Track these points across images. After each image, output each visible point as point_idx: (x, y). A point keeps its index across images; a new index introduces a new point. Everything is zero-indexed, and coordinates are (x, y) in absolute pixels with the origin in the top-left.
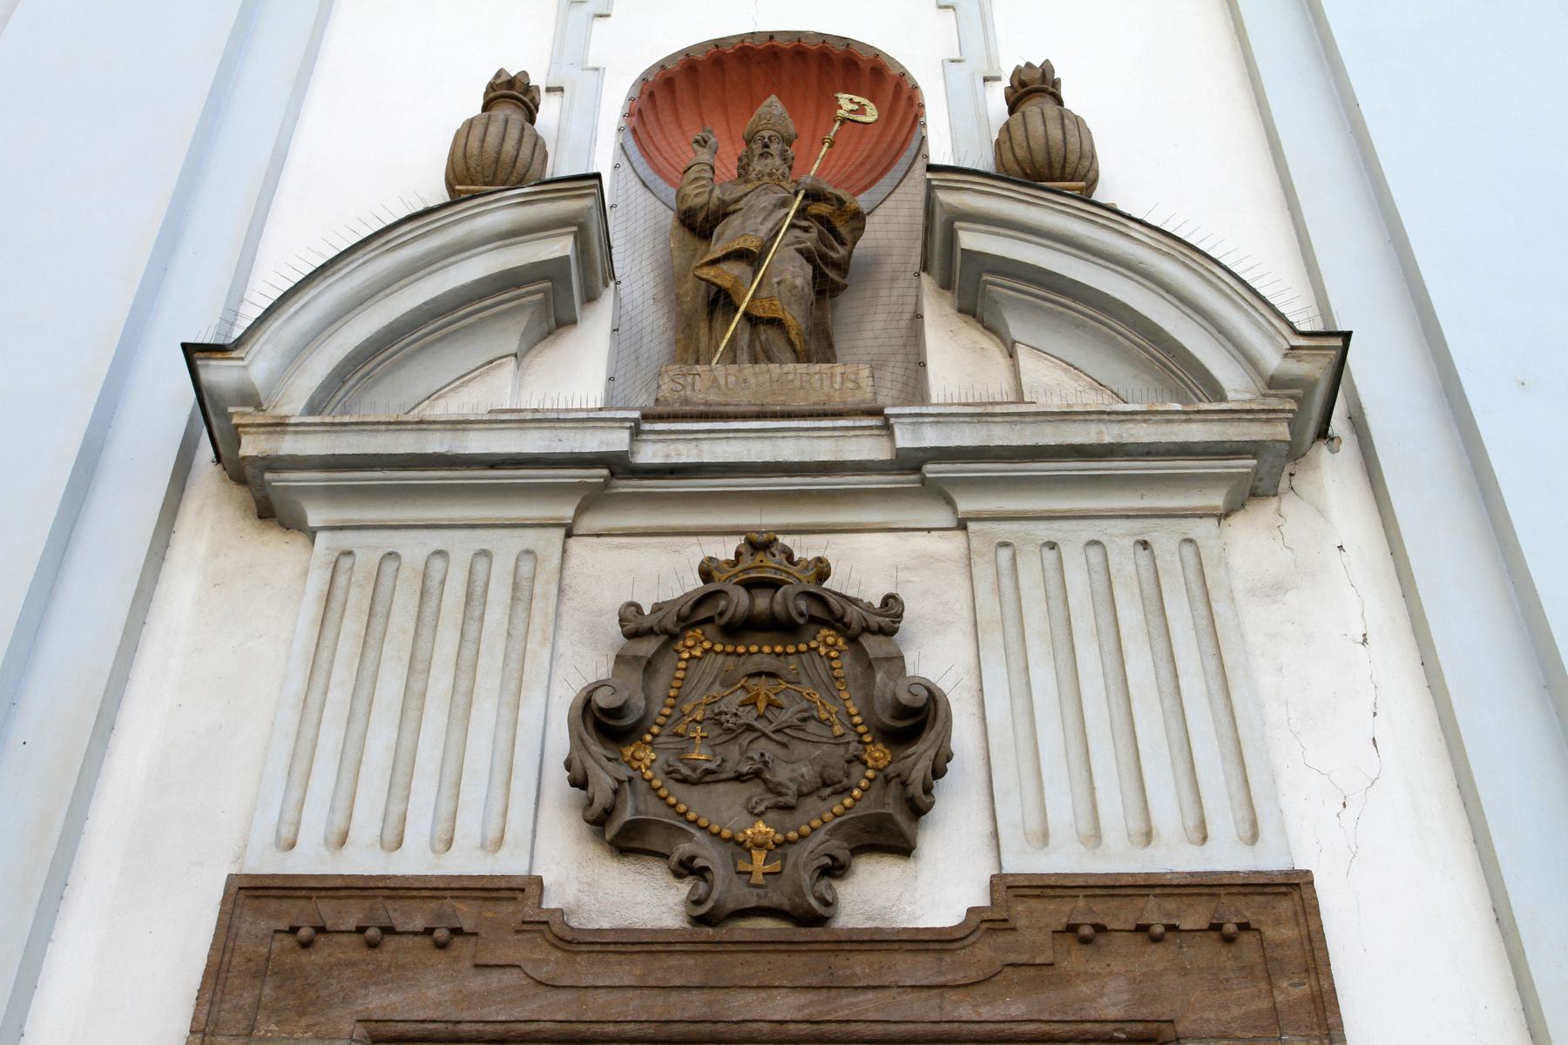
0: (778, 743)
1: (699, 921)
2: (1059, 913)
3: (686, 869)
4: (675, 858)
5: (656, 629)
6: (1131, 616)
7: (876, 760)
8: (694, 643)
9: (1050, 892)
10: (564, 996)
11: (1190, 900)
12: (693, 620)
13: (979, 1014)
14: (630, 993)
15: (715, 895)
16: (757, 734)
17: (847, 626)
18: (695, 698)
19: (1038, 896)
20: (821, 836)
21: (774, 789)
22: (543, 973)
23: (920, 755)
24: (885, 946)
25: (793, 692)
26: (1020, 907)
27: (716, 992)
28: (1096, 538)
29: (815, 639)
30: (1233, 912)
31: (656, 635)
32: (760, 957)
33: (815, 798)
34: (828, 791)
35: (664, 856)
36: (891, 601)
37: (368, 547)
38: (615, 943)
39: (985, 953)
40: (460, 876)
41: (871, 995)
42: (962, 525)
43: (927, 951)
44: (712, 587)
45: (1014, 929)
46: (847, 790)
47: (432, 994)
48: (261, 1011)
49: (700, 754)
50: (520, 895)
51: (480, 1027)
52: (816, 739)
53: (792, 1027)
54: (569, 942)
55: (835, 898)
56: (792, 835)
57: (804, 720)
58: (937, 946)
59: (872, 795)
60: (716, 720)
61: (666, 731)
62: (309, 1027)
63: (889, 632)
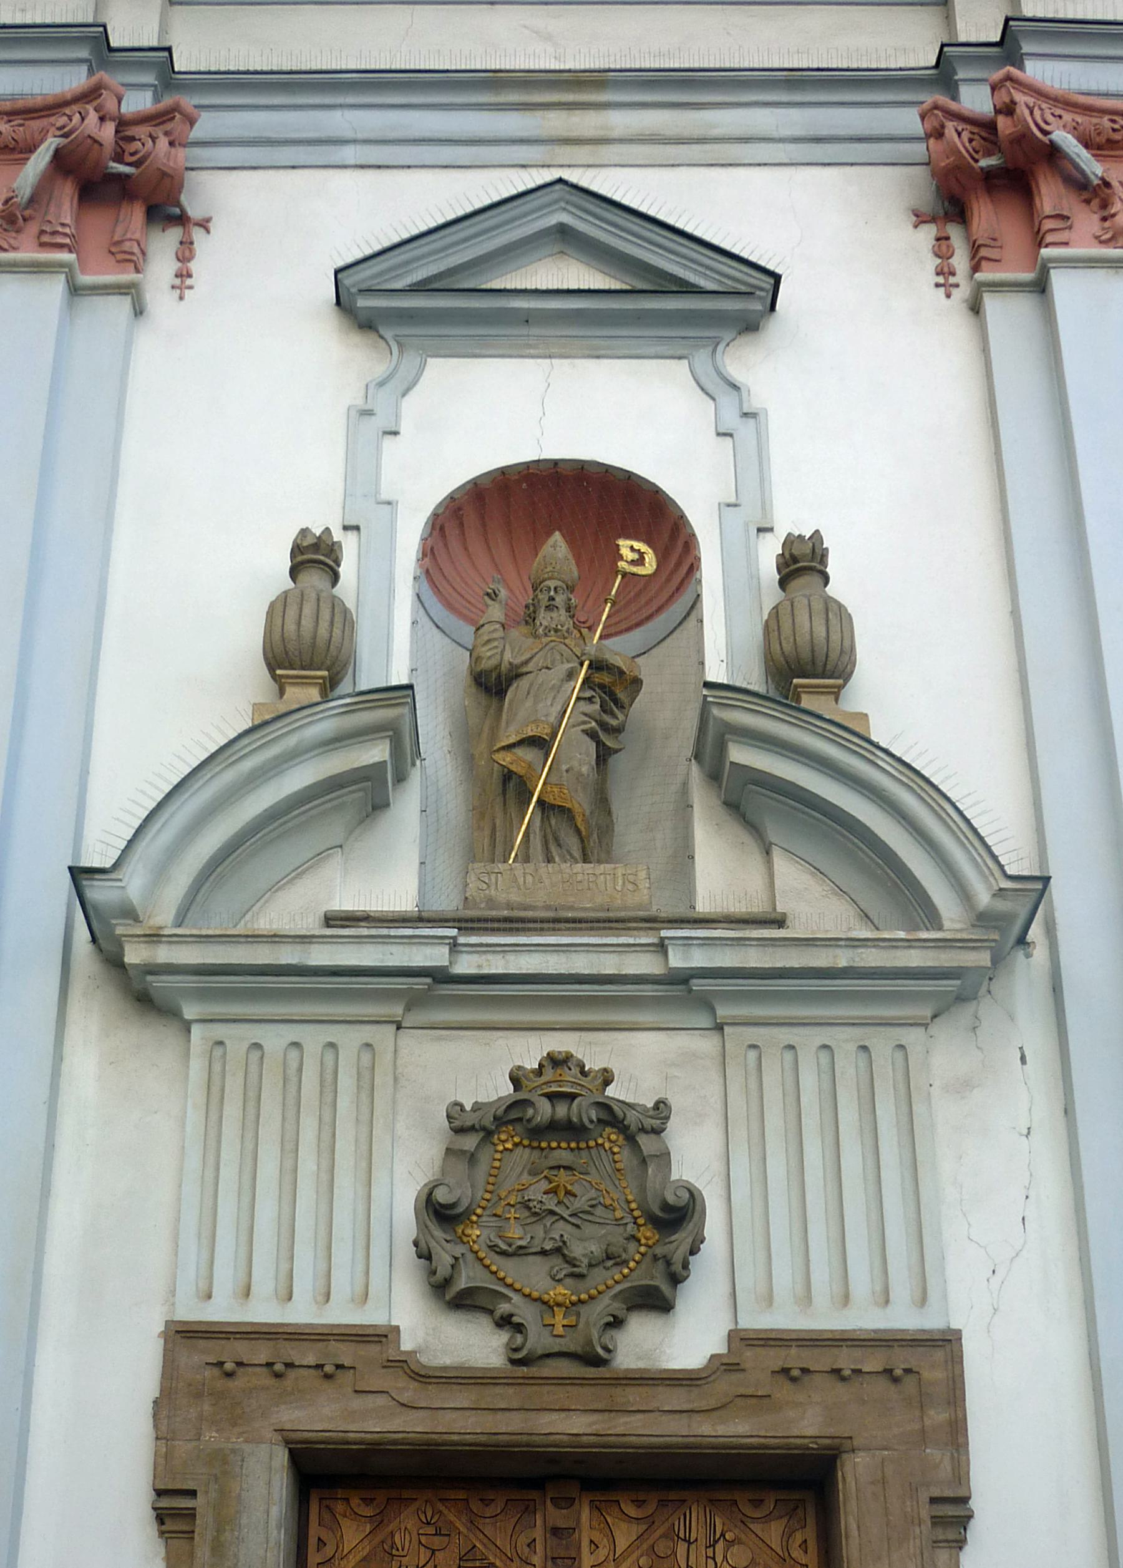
0: (573, 1224)
1: (513, 1362)
2: (775, 1359)
3: (505, 1322)
4: (498, 1314)
5: (477, 1126)
6: (849, 1115)
7: (647, 1239)
8: (506, 1139)
9: (772, 1343)
10: (421, 1414)
11: (870, 1350)
12: (505, 1120)
13: (716, 1431)
14: (468, 1413)
15: (528, 1345)
16: (557, 1217)
17: (627, 1128)
18: (508, 1185)
19: (763, 1346)
20: (606, 1300)
21: (571, 1262)
22: (405, 1398)
23: (682, 1238)
24: (651, 1382)
25: (584, 1182)
26: (748, 1353)
27: (530, 1413)
28: (828, 1043)
29: (601, 1136)
30: (900, 1360)
31: (477, 1131)
32: (561, 1388)
33: (601, 1267)
34: (610, 1263)
35: (491, 1312)
36: (662, 1105)
37: (238, 1037)
38: (457, 1377)
39: (725, 1386)
40: (339, 1325)
41: (640, 1416)
42: (719, 1028)
43: (681, 1385)
44: (521, 1096)
45: (743, 1370)
46: (625, 1263)
47: (326, 1411)
48: (204, 1422)
49: (515, 1232)
50: (384, 1340)
51: (363, 1435)
52: (602, 1221)
53: (585, 1438)
54: (423, 1376)
55: (615, 1347)
56: (584, 1296)
57: (592, 1206)
58: (688, 1382)
59: (643, 1266)
60: (526, 1205)
61: (488, 1212)
62: (240, 1434)
63: (657, 1132)
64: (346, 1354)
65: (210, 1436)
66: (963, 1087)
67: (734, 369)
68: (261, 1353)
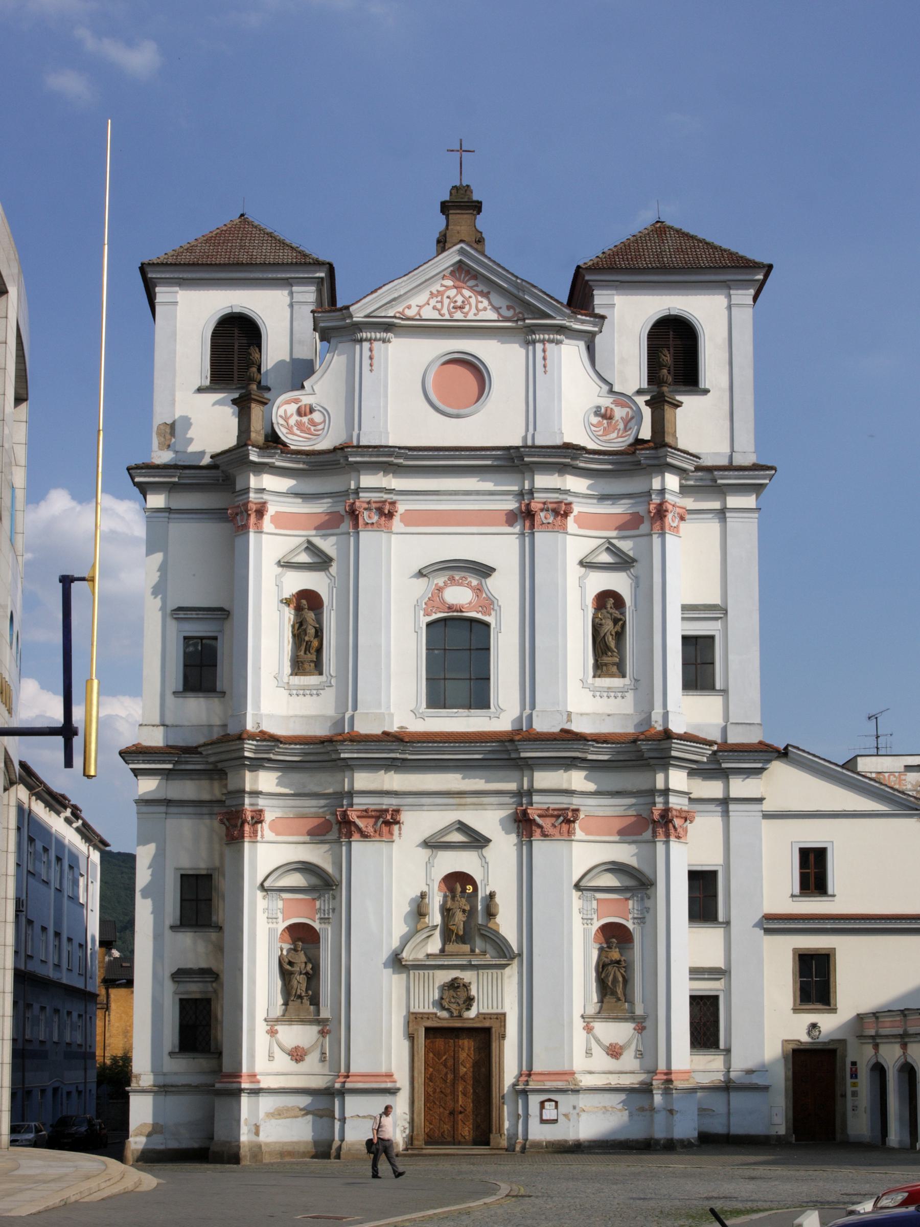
39: (477, 1019)
60: (453, 997)
65: (415, 1027)
68: (421, 1016)
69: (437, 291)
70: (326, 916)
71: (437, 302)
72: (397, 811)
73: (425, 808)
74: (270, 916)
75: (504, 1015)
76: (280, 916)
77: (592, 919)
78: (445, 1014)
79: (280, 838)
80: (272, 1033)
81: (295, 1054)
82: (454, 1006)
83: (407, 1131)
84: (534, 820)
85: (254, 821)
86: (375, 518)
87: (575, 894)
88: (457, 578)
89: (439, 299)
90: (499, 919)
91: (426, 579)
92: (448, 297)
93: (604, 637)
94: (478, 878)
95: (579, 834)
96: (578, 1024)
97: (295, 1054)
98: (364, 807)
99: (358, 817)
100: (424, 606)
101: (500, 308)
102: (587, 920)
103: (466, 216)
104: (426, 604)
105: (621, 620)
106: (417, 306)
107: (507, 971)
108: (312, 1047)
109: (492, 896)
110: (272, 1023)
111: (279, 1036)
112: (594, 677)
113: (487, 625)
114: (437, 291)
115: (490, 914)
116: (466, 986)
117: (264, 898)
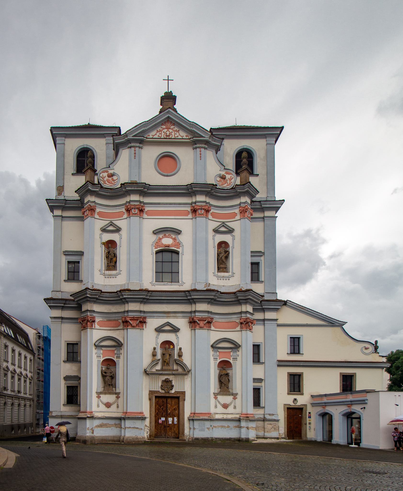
30: (183, 393)
39: (175, 394)
64: (157, 392)
66: (187, 378)
67: (177, 334)
69: (160, 130)
70: (118, 356)
71: (160, 134)
72: (145, 318)
73: (155, 317)
74: (98, 356)
75: (185, 392)
76: (102, 356)
77: (217, 359)
78: (163, 392)
79: (101, 328)
80: (99, 397)
81: (107, 405)
82: (166, 388)
83: (149, 433)
84: (196, 321)
85: (91, 321)
86: (137, 211)
87: (211, 349)
88: (167, 235)
89: (160, 133)
90: (183, 358)
91: (155, 235)
92: (164, 132)
93: (221, 258)
94: (175, 343)
95: (213, 328)
96: (212, 396)
97: (107, 405)
98: (133, 316)
99: (130, 320)
100: (155, 245)
101: (183, 136)
102: (215, 359)
103: (170, 102)
104: (155, 244)
105: (227, 252)
106: (152, 135)
107: (186, 377)
108: (114, 403)
109: (180, 349)
110: (99, 394)
111: (101, 398)
112: (218, 272)
113: (177, 253)
114: (160, 130)
115: (180, 356)
116: (171, 381)
117: (95, 349)
